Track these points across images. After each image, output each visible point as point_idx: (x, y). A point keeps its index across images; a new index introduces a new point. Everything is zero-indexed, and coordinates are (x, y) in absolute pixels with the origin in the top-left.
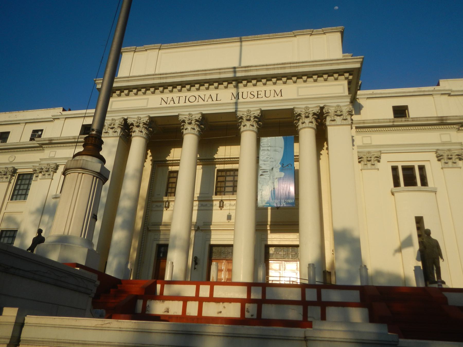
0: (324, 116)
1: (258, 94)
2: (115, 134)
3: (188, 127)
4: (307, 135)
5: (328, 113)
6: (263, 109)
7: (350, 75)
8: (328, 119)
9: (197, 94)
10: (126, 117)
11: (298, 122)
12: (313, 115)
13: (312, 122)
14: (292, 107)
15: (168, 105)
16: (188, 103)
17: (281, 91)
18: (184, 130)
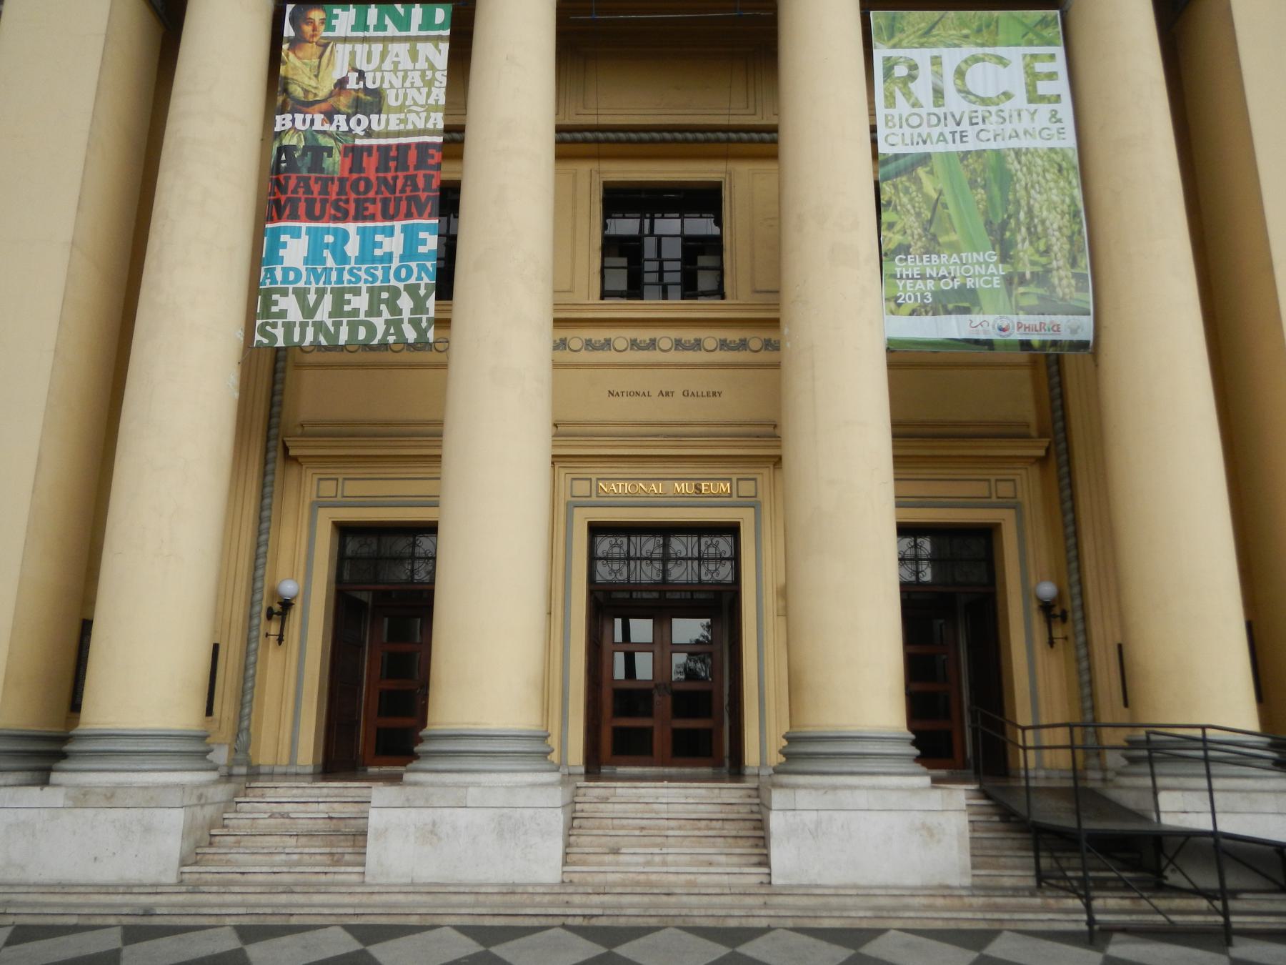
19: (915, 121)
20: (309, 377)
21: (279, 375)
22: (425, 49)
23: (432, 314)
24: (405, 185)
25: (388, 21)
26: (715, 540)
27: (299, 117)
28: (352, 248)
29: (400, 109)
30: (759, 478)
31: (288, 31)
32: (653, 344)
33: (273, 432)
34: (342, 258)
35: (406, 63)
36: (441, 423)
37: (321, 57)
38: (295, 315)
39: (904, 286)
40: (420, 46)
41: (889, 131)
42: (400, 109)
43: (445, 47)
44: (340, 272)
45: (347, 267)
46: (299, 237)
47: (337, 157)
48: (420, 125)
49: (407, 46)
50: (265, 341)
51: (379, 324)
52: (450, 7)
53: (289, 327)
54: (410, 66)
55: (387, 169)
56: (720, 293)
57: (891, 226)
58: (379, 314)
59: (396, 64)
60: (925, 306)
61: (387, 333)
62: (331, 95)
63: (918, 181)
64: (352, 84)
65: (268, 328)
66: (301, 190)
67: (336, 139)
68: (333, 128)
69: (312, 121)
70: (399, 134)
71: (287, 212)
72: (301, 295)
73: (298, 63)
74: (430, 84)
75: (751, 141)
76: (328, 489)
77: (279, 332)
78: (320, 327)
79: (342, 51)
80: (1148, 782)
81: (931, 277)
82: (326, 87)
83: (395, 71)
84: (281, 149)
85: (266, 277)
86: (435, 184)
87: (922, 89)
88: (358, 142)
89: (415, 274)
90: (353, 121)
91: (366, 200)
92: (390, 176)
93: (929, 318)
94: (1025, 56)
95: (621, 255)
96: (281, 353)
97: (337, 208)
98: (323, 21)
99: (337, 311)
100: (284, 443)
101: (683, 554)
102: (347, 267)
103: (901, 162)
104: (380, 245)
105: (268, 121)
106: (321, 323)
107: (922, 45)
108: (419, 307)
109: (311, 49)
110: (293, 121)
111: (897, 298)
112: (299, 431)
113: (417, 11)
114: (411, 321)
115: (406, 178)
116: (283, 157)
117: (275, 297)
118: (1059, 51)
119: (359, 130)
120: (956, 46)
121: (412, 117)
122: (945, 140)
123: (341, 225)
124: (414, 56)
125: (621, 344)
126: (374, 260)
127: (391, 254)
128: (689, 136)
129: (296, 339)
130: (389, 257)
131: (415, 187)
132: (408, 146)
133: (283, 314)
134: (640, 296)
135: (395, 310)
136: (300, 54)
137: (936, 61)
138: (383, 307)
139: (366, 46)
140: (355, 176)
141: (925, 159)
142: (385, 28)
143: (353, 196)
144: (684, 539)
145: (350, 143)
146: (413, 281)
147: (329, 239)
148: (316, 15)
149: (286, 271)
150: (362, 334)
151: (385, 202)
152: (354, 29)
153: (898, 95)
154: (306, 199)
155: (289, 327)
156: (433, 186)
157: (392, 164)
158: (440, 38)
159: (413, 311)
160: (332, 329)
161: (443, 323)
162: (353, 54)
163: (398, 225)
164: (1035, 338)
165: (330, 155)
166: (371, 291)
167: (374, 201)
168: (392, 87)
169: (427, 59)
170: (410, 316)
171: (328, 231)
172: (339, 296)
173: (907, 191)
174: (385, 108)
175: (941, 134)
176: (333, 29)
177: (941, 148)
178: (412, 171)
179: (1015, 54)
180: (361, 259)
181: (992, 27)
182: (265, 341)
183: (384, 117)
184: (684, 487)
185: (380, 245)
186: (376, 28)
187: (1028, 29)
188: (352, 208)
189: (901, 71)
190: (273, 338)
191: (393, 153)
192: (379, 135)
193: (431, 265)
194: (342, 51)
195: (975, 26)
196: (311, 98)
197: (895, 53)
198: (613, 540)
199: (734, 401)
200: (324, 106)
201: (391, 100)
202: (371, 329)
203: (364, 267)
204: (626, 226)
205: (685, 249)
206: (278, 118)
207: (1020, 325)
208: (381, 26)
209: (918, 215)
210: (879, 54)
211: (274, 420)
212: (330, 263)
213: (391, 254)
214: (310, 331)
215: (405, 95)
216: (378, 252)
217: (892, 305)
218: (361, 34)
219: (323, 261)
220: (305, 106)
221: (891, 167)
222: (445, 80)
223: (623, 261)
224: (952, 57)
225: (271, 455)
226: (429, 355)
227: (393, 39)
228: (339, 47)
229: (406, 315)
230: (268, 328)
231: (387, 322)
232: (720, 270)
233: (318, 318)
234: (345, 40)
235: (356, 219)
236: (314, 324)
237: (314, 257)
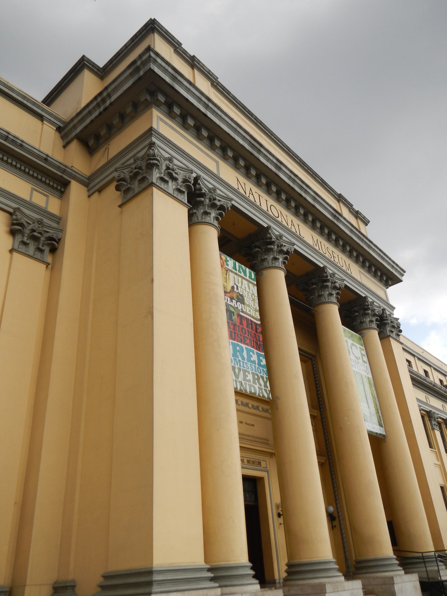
0: (386, 321)
8: (388, 328)
28: (245, 354)
29: (248, 306)
34: (243, 358)
35: (247, 289)
37: (226, 275)
43: (256, 288)
58: (256, 384)
62: (231, 292)
64: (235, 290)
80: (436, 568)
88: (241, 313)
99: (245, 379)
113: (248, 270)
114: (264, 389)
119: (240, 308)
138: (256, 381)
142: (241, 273)
165: (234, 315)
172: (245, 371)
176: (228, 265)
203: (249, 363)
212: (240, 359)
219: (238, 357)
228: (230, 273)
229: (263, 387)
234: (232, 271)
236: (239, 381)
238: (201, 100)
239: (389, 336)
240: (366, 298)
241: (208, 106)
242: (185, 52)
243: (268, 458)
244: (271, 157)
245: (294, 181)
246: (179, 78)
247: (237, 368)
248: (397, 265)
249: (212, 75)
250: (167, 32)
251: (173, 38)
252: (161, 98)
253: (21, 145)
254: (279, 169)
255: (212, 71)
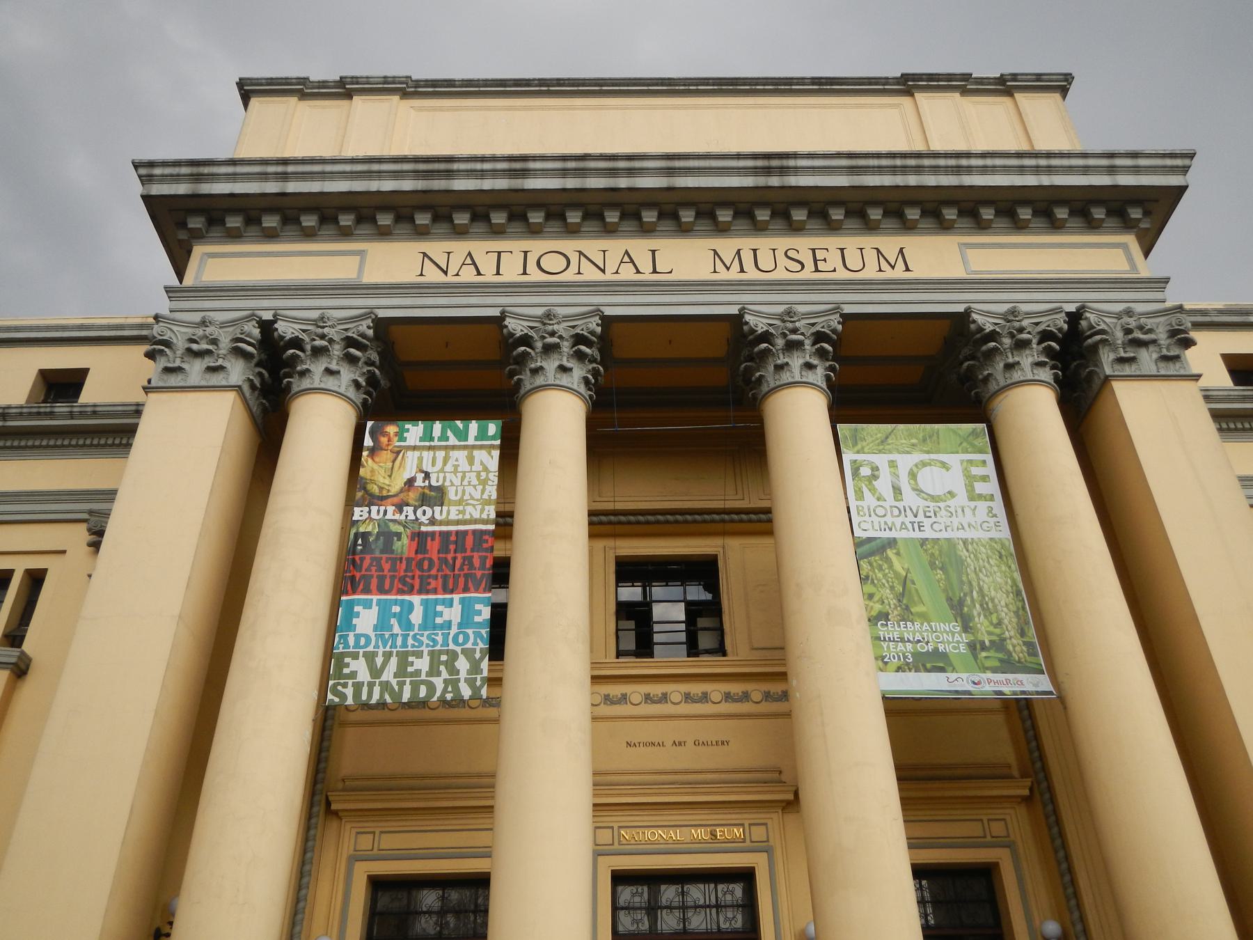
0: (1090, 341)
1: (815, 261)
2: (217, 379)
3: (544, 364)
4: (1034, 409)
5: (1102, 332)
6: (848, 309)
7: (1147, 213)
8: (1107, 358)
9: (570, 246)
10: (267, 316)
11: (982, 367)
12: (1039, 343)
13: (1040, 364)
14: (960, 308)
15: (450, 279)
16: (535, 276)
17: (901, 250)
18: (526, 376)
19: (880, 511)
20: (351, 732)
21: (327, 733)
22: (480, 455)
23: (485, 674)
24: (463, 564)
25: (449, 433)
26: (731, 886)
27: (374, 509)
28: (416, 617)
29: (460, 502)
30: (769, 822)
31: (368, 442)
32: (664, 698)
33: (319, 786)
34: (408, 626)
35: (464, 465)
36: (493, 776)
37: (394, 462)
38: (364, 675)
39: (888, 647)
40: (476, 453)
41: (862, 519)
42: (460, 502)
43: (496, 453)
44: (405, 637)
45: (412, 633)
46: (370, 608)
47: (405, 540)
48: (476, 515)
49: (466, 452)
50: (337, 700)
51: (439, 683)
52: (500, 422)
53: (358, 687)
54: (467, 468)
55: (448, 551)
56: (721, 650)
57: (871, 596)
58: (439, 674)
59: (456, 467)
60: (908, 664)
61: (445, 691)
62: (401, 491)
63: (888, 560)
64: (419, 482)
65: (339, 688)
66: (374, 569)
67: (405, 527)
68: (403, 517)
69: (385, 512)
70: (458, 522)
71: (361, 587)
72: (369, 658)
73: (375, 467)
74: (484, 483)
75: (741, 521)
76: (365, 842)
77: (349, 692)
78: (386, 686)
79: (412, 457)
81: (909, 641)
82: (397, 484)
83: (455, 472)
84: (356, 535)
85: (339, 643)
86: (489, 563)
87: (884, 484)
88: (423, 529)
89: (472, 640)
90: (419, 512)
91: (429, 576)
92: (450, 556)
93: (912, 674)
94: (962, 462)
95: (628, 619)
96: (330, 712)
97: (404, 582)
98: (396, 434)
99: (401, 672)
100: (327, 797)
101: (702, 902)
102: (412, 633)
103: (873, 544)
104: (441, 614)
105: (348, 512)
106: (387, 682)
107: (880, 452)
108: (475, 668)
109: (386, 456)
110: (370, 512)
111: (883, 658)
112: (340, 785)
113: (474, 426)
114: (466, 680)
115: (464, 559)
116: (360, 542)
117: (347, 660)
118: (989, 458)
119: (424, 519)
120: (908, 453)
121: (469, 509)
122: (906, 528)
123: (407, 597)
124: (471, 460)
125: (636, 698)
126: (435, 627)
127: (450, 622)
128: (689, 517)
129: (364, 697)
130: (448, 624)
131: (471, 566)
132: (466, 532)
133: (353, 675)
134: (651, 655)
135: (453, 671)
136: (377, 459)
137: (892, 464)
138: (442, 668)
139: (431, 453)
140: (420, 556)
141: (892, 543)
142: (447, 439)
143: (418, 573)
144: (702, 886)
145: (417, 530)
146: (469, 645)
147: (396, 609)
148: (391, 429)
149: (358, 637)
150: (423, 692)
151: (445, 577)
152: (421, 439)
153: (865, 490)
154: (378, 577)
155: (358, 687)
156: (493, 565)
157: (452, 547)
158: (492, 447)
159: (469, 672)
160: (396, 688)
161: (495, 682)
162: (421, 459)
163: (456, 597)
164: (1006, 689)
165: (399, 539)
166: (431, 653)
167: (436, 578)
168: (452, 485)
169: (482, 463)
170: (467, 677)
171: (396, 602)
172: (403, 659)
173: (880, 569)
174: (446, 502)
175: (903, 523)
176: (405, 440)
177: (903, 534)
178: (468, 553)
179: (954, 460)
180: (424, 627)
181: (935, 438)
182: (337, 700)
183: (445, 508)
184: (701, 834)
185: (441, 614)
186: (440, 439)
187: (966, 439)
188: (417, 587)
189: (865, 471)
190: (343, 696)
191: (453, 538)
192: (441, 523)
193: (485, 632)
194: (412, 457)
195: (921, 436)
196: (385, 493)
197: (860, 457)
198: (634, 889)
199: (741, 747)
200: (395, 500)
201: (452, 495)
202: (431, 688)
204: (631, 593)
205: (688, 612)
206: (357, 510)
207: (989, 681)
208: (444, 437)
209: (892, 588)
210: (847, 457)
211: (320, 776)
212: (396, 629)
213: (450, 622)
214: (377, 689)
215: (464, 491)
216: (438, 620)
217: (880, 663)
218: (427, 444)
219: (391, 628)
220: (381, 499)
221: (866, 548)
222: (496, 480)
223: (631, 624)
224: (906, 462)
225: (315, 809)
226: (486, 709)
227: (454, 447)
228: (410, 453)
229: (463, 675)
230: (339, 688)
231: (445, 681)
232: (720, 631)
233: (384, 678)
234: (414, 448)
235: (420, 592)
236: (381, 683)
237: (382, 625)
238: (266, 174)
239: (1107, 379)
240: (968, 313)
241: (286, 173)
242: (323, 84)
243: (774, 816)
244: (487, 166)
245: (582, 173)
246: (206, 170)
247: (380, 654)
248: (1134, 155)
249: (394, 80)
250: (271, 81)
251: (286, 81)
252: (196, 223)
253: (94, 412)
254: (525, 173)
255: (390, 73)
